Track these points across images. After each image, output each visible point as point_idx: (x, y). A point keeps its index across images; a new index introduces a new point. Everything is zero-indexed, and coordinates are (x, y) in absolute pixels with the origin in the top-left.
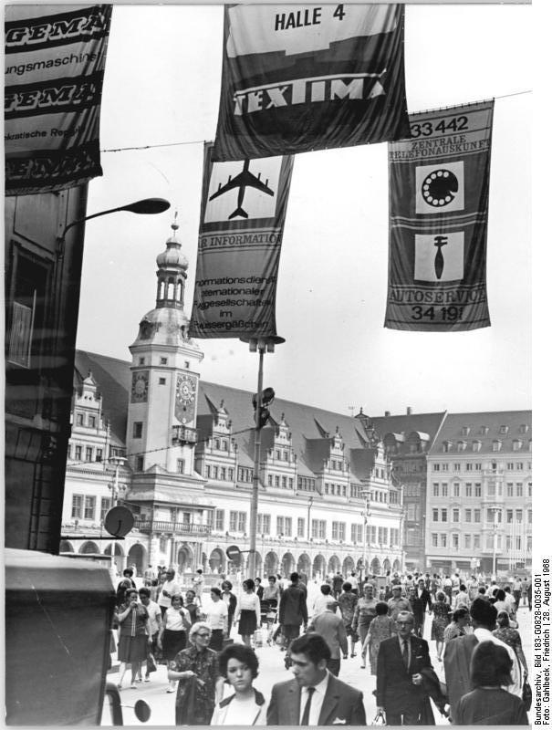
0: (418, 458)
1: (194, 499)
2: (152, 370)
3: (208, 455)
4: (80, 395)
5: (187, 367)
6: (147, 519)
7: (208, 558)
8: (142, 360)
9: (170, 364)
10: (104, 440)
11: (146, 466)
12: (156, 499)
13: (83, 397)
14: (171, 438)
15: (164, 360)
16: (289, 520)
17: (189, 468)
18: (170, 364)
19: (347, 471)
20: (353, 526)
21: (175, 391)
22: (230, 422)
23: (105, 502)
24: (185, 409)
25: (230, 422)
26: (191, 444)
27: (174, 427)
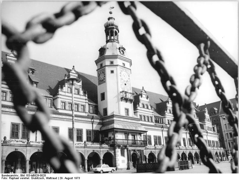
1: (136, 127)
2: (107, 67)
5: (124, 65)
6: (112, 139)
7: (147, 157)
8: (101, 65)
9: (115, 64)
11: (109, 113)
15: (112, 63)
17: (131, 113)
18: (115, 64)
19: (197, 118)
21: (119, 76)
22: (148, 96)
23: (88, 132)
25: (148, 96)
26: (131, 101)
27: (121, 92)
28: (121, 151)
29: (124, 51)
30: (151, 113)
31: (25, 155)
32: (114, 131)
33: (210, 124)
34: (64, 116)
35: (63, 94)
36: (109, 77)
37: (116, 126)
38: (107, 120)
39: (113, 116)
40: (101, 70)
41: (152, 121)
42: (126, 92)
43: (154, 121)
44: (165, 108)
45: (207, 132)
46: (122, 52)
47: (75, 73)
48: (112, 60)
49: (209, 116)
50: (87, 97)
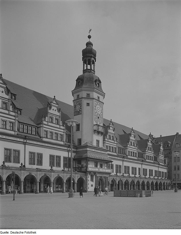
0: (167, 150)
3: (107, 141)
4: (50, 108)
7: (110, 183)
8: (78, 96)
10: (63, 131)
12: (88, 157)
13: (52, 109)
14: (93, 130)
16: (136, 168)
19: (153, 151)
20: (155, 171)
22: (114, 129)
23: (64, 158)
24: (98, 118)
25: (114, 129)
26: (102, 133)
28: (91, 177)
29: (99, 83)
30: (113, 144)
31: (36, 177)
32: (87, 159)
33: (163, 157)
34: (46, 144)
35: (46, 123)
36: (86, 109)
37: (90, 155)
38: (81, 150)
39: (86, 146)
40: (78, 100)
41: (115, 152)
42: (99, 126)
43: (117, 151)
44: (128, 140)
45: (159, 164)
46: (98, 85)
47: (55, 103)
48: (88, 92)
49: (163, 149)
50: (65, 127)
